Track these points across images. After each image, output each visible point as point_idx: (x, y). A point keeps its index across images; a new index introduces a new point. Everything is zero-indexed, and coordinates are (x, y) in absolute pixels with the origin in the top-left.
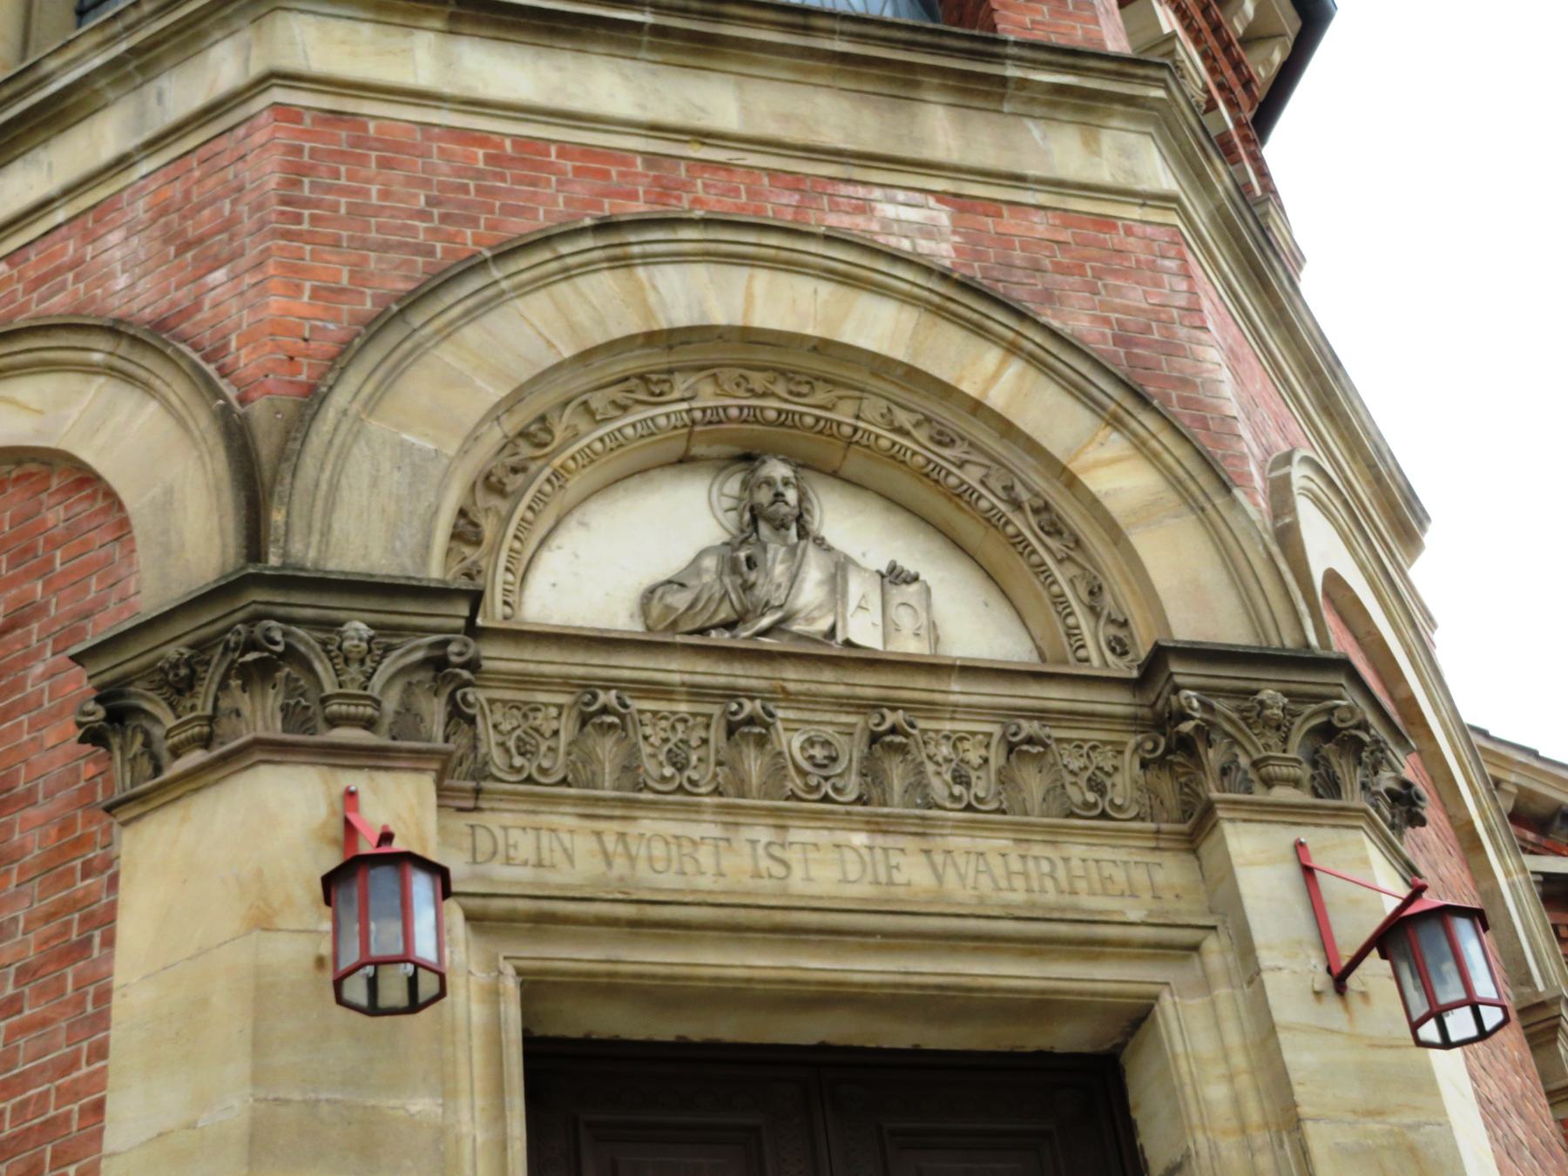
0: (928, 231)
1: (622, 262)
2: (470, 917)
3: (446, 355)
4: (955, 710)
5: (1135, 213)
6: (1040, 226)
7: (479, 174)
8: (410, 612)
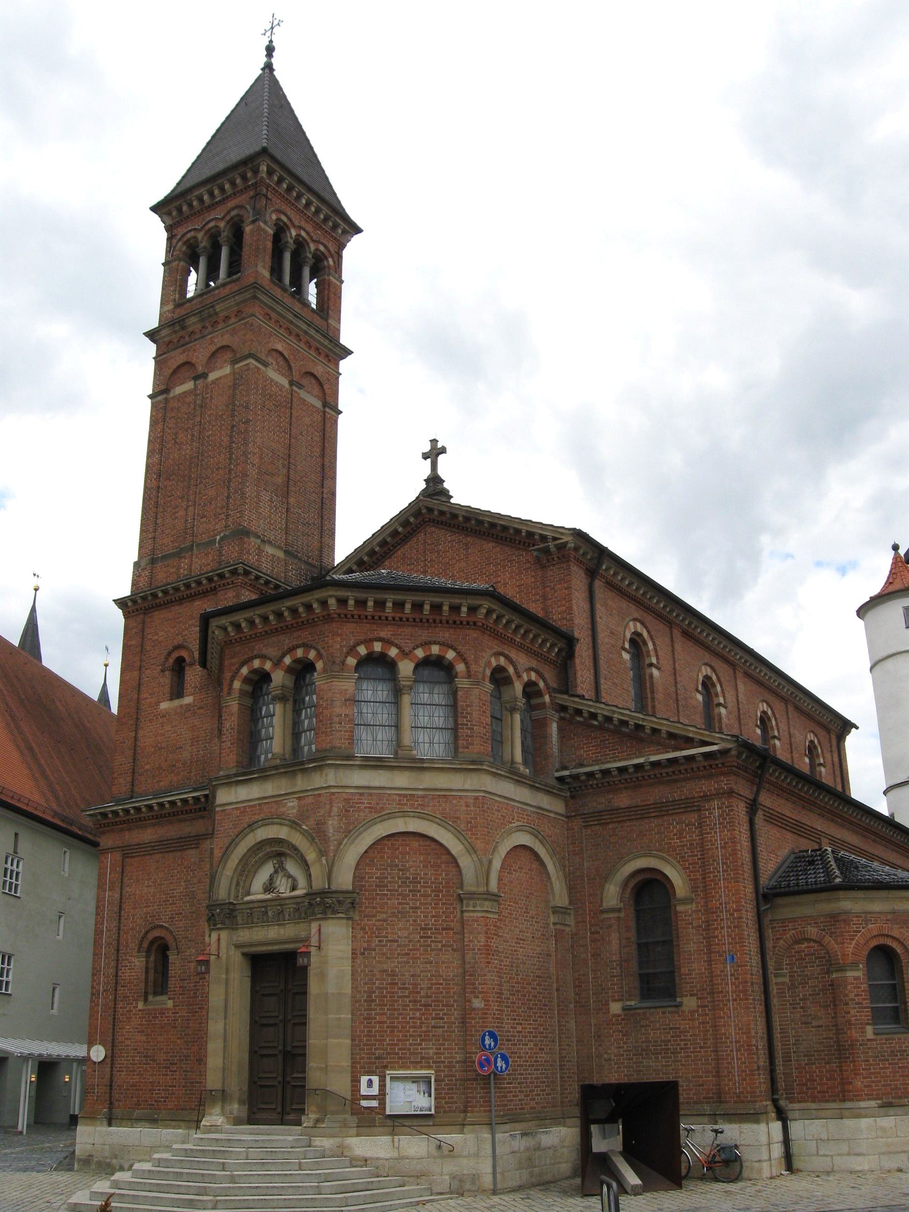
0: (293, 808)
1: (253, 831)
2: (235, 947)
3: (233, 856)
4: (288, 904)
5: (324, 791)
6: (310, 800)
7: (238, 817)
8: (223, 907)
